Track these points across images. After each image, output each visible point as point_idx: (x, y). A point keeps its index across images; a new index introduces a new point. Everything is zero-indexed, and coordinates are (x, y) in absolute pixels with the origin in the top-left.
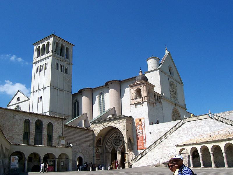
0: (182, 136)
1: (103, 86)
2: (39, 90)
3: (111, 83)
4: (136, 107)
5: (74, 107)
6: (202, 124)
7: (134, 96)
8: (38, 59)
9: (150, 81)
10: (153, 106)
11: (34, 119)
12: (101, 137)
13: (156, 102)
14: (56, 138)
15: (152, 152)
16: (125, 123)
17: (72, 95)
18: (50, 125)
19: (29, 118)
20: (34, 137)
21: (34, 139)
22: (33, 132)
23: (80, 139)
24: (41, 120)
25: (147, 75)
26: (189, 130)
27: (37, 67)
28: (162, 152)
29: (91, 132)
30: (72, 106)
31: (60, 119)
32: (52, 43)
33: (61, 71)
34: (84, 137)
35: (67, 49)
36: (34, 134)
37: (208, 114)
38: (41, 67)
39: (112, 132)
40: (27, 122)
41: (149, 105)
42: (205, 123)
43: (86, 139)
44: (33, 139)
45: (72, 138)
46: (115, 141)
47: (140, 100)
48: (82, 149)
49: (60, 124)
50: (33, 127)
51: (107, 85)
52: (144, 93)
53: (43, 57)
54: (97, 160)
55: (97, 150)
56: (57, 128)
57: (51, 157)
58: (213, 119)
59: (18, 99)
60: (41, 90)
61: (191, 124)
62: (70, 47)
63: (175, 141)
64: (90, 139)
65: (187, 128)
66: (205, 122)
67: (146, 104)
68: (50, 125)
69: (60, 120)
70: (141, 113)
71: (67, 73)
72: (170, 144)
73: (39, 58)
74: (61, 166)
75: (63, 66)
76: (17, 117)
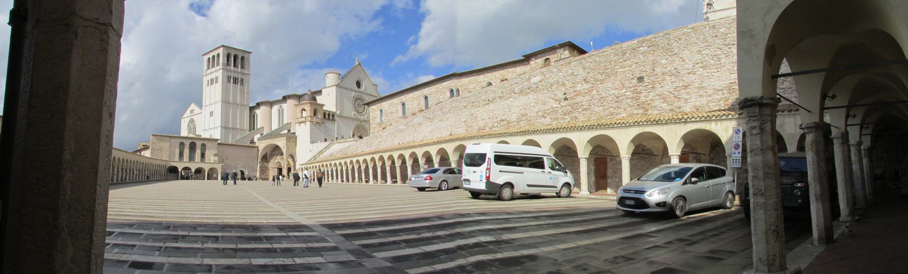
2: (211, 104)
8: (209, 71)
18: (203, 146)
19: (184, 141)
38: (212, 80)
40: (182, 144)
53: (214, 69)
59: (192, 111)
62: (246, 56)
68: (203, 146)
71: (242, 84)
76: (173, 140)
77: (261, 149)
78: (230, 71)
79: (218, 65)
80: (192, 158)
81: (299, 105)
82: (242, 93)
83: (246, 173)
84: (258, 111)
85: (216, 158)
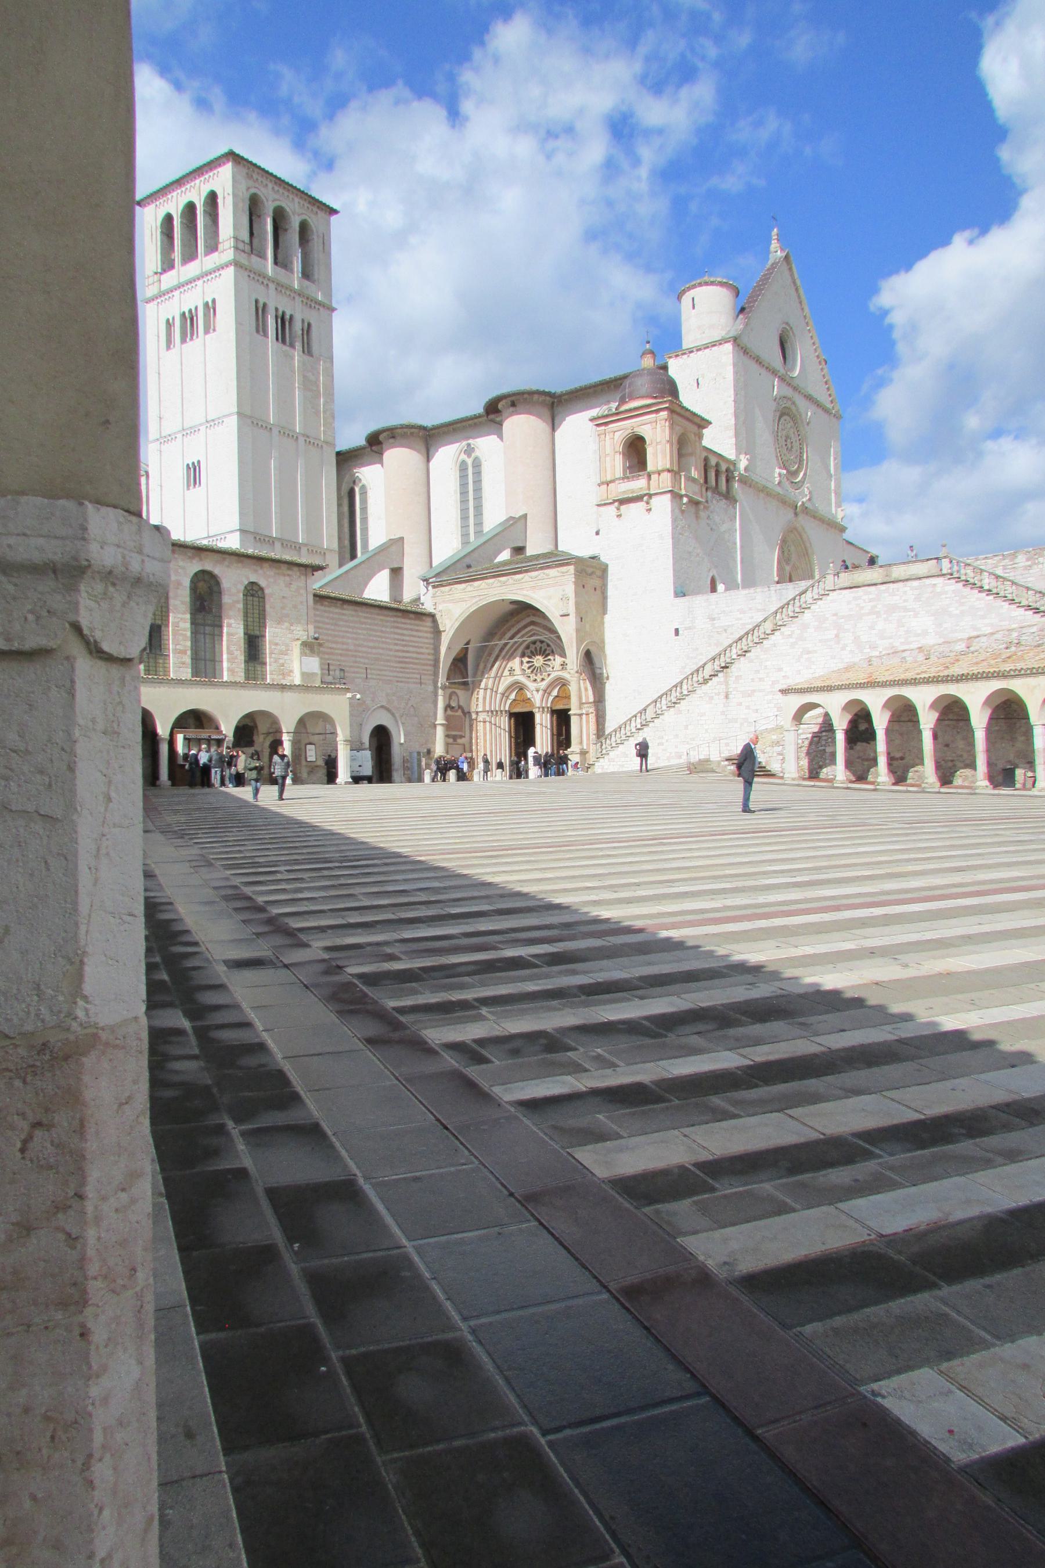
0: (815, 652)
1: (476, 417)
2: (187, 431)
3: (513, 404)
4: (619, 516)
5: (346, 509)
6: (905, 601)
7: (617, 464)
8: (170, 279)
9: (688, 399)
10: (697, 517)
11: (183, 568)
12: (468, 643)
13: (709, 494)
14: (283, 648)
15: (680, 712)
16: (570, 589)
17: (338, 454)
18: (254, 592)
20: (189, 643)
21: (189, 653)
22: (182, 625)
23: (381, 651)
24: (217, 571)
25: (677, 369)
26: (846, 627)
27: (168, 321)
28: (723, 713)
29: (428, 623)
30: (339, 505)
31: (296, 569)
32: (230, 200)
33: (284, 342)
34: (396, 644)
35: (304, 227)
36: (189, 634)
37: (937, 558)
38: (189, 320)
39: (518, 622)
41: (677, 511)
42: (918, 599)
43: (404, 651)
44: (184, 652)
45: (345, 647)
46: (528, 662)
47: (638, 484)
48: (387, 695)
49: (294, 587)
50: (183, 603)
51: (494, 412)
52: (659, 454)
53: (193, 269)
54: (451, 740)
55: (450, 698)
56: (283, 608)
57: (263, 727)
58: (953, 581)
60: (194, 430)
61: (856, 599)
62: (315, 221)
63: (780, 670)
64: (422, 653)
65: (835, 615)
66: (916, 592)
67: (663, 505)
68: (254, 592)
69: (295, 572)
70: (639, 542)
71: (307, 350)
72: (761, 680)
73: (172, 273)
74: (304, 763)
75: (291, 317)
77: (449, 625)
78: (259, 276)
79: (213, 247)
80: (204, 665)
81: (618, 416)
82: (310, 386)
83: (399, 738)
84: (368, 475)
85: (314, 664)
